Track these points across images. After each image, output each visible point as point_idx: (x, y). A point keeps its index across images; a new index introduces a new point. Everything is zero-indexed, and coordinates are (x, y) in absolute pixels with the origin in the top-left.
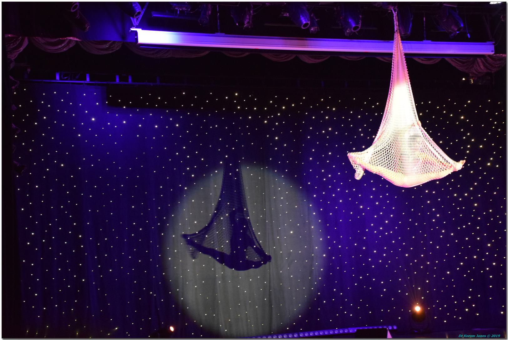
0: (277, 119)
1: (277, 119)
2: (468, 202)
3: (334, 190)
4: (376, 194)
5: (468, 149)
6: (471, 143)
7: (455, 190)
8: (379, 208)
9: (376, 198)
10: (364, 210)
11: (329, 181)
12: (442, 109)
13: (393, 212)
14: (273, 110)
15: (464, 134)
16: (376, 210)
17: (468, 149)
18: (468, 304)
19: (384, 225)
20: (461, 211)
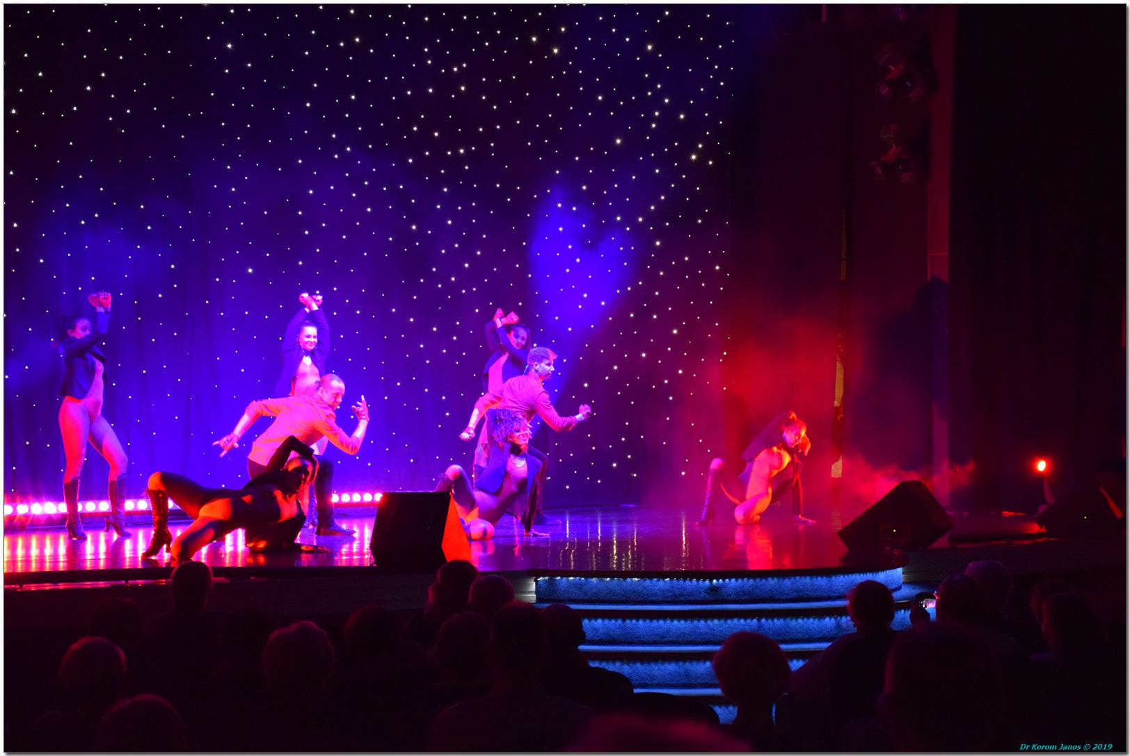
3: (355, 184)
4: (449, 201)
5: (655, 120)
6: (662, 107)
9: (449, 211)
10: (420, 234)
11: (347, 160)
17: (655, 120)
18: (618, 455)
19: (460, 272)
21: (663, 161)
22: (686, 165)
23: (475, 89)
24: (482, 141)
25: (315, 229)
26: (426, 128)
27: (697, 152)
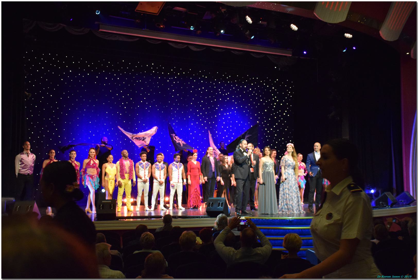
0: (174, 80)
1: (174, 80)
2: (272, 133)
3: (202, 122)
5: (275, 105)
7: (266, 126)
8: (226, 133)
9: (225, 128)
12: (263, 82)
13: (233, 136)
14: (172, 75)
15: (274, 97)
16: (224, 134)
20: (268, 138)
21: (277, 115)
22: (283, 116)
23: (231, 99)
24: (233, 111)
25: (193, 133)
26: (219, 108)
27: (285, 113)
